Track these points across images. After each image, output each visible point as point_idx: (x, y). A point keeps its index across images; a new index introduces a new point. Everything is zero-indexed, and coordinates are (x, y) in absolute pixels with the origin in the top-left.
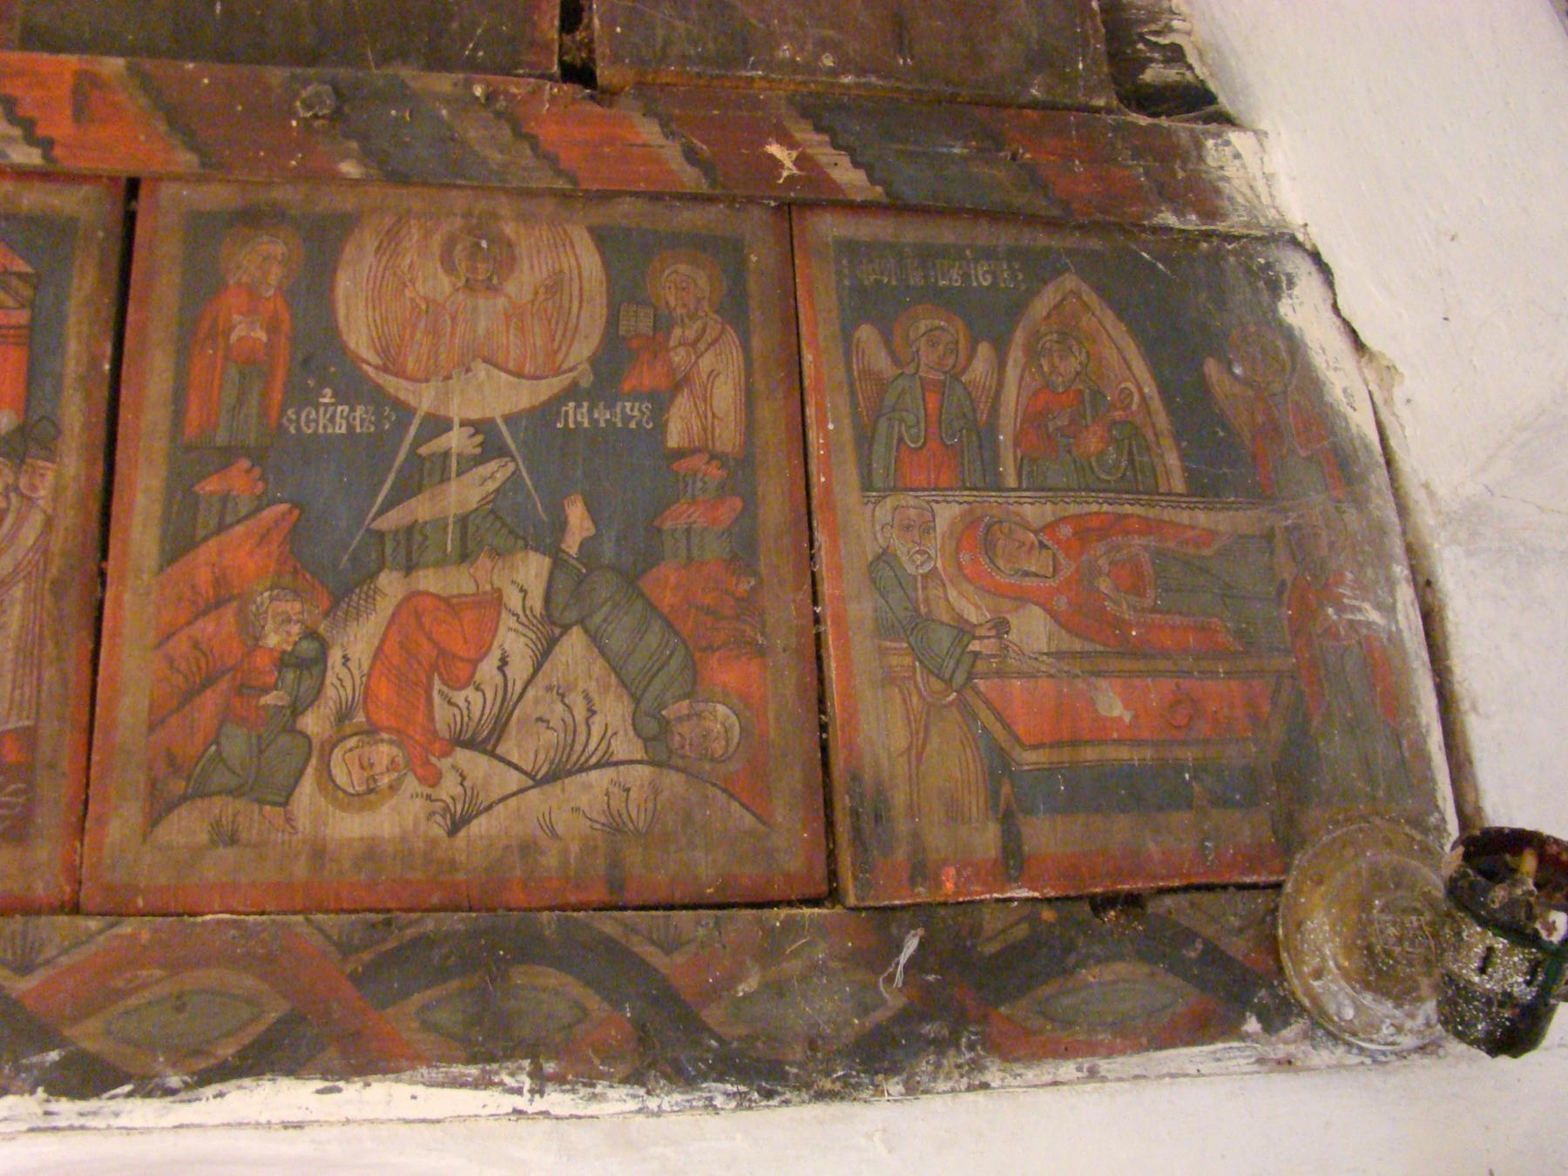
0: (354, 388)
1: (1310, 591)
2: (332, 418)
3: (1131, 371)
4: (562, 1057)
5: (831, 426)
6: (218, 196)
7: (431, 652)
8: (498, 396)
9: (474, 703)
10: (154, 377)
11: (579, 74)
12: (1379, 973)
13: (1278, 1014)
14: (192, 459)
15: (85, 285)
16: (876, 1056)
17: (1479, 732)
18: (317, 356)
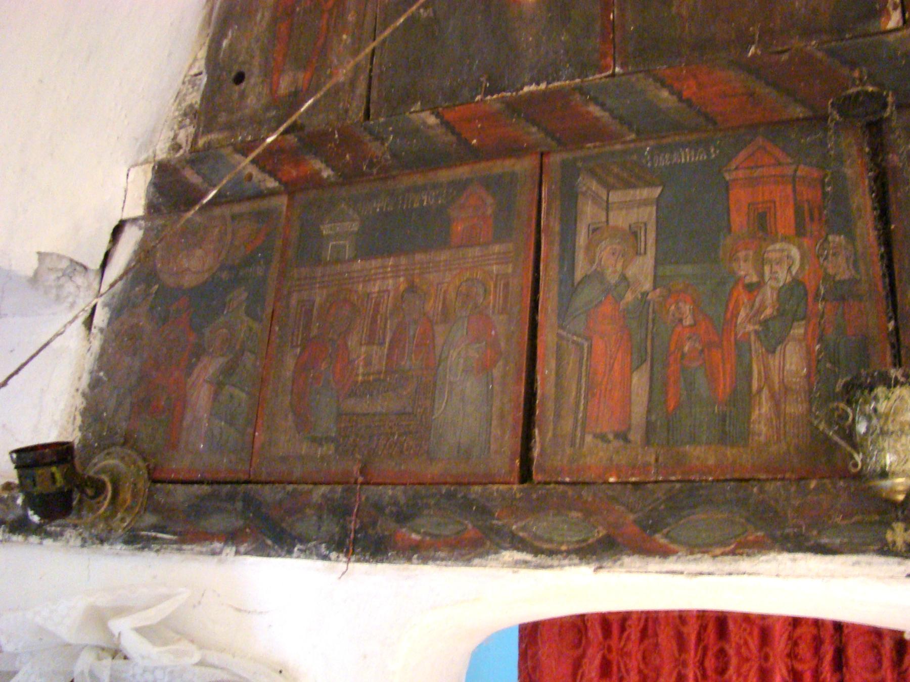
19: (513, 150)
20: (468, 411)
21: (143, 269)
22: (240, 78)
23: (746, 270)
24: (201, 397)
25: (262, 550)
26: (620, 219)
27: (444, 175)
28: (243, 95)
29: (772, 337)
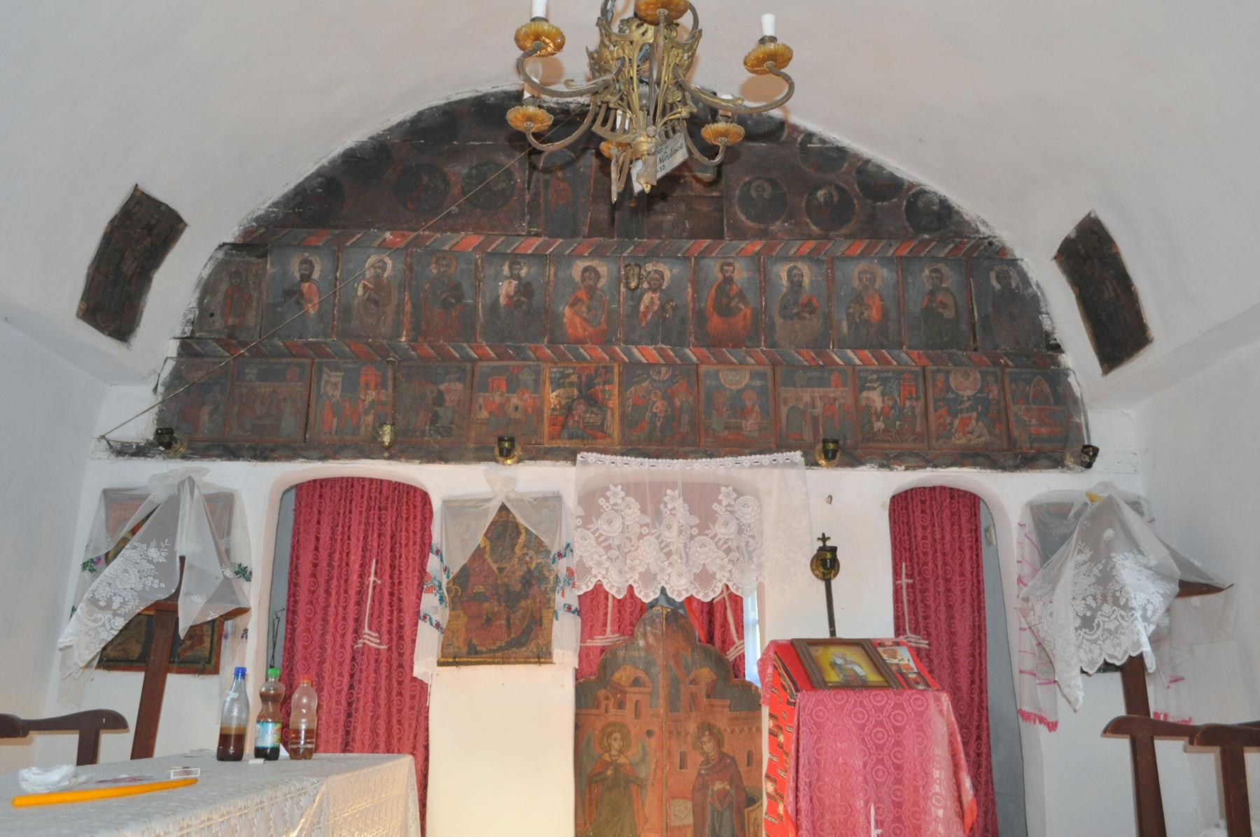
0: (953, 392)
1: (1070, 417)
2: (951, 396)
3: (1047, 389)
4: (983, 466)
5: (1009, 397)
6: (935, 368)
7: (965, 423)
8: (969, 393)
9: (970, 429)
10: (931, 391)
11: (975, 350)
12: (1076, 463)
13: (1063, 466)
14: (935, 402)
15: (920, 380)
16: (1016, 468)
17: (1092, 435)
18: (948, 388)
20: (290, 425)
21: (177, 375)
22: (212, 315)
23: (362, 397)
24: (205, 417)
26: (333, 380)
27: (284, 360)
29: (366, 413)
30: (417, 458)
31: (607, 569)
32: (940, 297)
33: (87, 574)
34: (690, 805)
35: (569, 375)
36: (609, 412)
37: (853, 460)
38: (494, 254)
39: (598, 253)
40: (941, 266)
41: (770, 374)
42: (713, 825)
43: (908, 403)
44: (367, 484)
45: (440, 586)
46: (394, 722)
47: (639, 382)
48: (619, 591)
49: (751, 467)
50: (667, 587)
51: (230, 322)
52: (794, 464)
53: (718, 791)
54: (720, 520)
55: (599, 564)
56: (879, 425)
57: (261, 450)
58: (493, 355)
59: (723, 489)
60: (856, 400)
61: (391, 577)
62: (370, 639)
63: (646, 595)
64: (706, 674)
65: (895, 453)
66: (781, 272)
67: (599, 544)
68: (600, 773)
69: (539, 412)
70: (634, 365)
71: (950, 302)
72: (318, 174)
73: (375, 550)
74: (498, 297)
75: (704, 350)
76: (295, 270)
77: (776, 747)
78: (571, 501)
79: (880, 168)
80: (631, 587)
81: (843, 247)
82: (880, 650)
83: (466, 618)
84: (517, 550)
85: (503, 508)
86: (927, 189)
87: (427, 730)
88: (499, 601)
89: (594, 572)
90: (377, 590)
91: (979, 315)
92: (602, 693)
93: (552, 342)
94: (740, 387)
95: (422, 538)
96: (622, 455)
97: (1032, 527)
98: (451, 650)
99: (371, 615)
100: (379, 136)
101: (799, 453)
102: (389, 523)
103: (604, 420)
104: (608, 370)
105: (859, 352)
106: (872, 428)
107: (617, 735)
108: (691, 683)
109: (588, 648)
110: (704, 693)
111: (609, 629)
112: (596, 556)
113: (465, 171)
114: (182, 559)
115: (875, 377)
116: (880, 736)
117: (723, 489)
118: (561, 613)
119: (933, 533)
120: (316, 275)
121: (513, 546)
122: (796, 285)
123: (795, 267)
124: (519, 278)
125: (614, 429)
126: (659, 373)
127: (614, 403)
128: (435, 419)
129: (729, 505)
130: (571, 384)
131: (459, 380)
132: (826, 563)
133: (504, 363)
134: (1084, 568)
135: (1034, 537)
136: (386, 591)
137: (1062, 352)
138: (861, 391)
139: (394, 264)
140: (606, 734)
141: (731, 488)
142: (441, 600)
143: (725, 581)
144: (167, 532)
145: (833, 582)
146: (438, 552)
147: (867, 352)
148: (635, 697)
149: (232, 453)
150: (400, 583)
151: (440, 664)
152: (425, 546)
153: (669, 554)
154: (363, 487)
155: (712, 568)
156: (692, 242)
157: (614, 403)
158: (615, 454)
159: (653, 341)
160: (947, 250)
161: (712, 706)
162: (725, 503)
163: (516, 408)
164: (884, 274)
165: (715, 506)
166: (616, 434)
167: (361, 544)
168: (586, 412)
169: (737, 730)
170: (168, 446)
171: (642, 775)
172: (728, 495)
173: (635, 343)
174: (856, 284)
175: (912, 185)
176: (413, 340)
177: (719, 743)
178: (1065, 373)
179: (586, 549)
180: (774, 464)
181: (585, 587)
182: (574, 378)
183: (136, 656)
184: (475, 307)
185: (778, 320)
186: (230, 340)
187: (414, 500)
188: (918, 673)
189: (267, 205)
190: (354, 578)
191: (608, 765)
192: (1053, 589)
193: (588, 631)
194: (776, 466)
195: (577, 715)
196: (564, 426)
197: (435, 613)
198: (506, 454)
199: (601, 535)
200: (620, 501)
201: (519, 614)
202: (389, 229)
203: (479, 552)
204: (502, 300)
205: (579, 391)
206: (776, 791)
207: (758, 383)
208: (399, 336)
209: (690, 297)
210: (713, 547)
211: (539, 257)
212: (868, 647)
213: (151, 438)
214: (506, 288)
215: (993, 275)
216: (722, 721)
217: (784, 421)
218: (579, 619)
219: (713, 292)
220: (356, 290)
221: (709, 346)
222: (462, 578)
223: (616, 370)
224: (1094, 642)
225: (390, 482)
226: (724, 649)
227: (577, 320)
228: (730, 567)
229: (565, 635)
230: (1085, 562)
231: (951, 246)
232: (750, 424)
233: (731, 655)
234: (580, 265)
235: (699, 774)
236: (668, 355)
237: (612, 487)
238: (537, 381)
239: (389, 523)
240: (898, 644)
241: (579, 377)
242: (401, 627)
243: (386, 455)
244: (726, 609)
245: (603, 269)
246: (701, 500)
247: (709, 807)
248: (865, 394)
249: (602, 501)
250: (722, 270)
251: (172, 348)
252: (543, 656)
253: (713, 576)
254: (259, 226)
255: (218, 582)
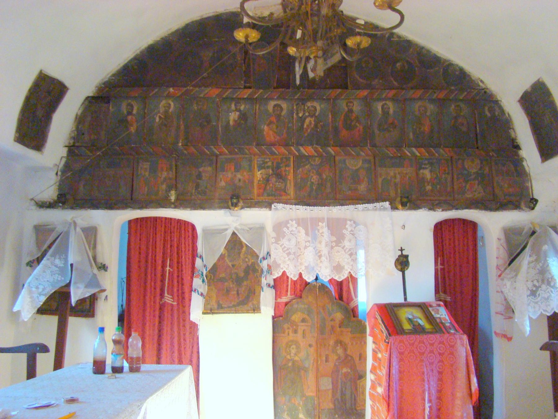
0: (466, 169)
2: (465, 172)
4: (481, 209)
5: (494, 172)
7: (472, 186)
8: (475, 171)
11: (478, 148)
12: (526, 207)
16: (496, 209)
17: (534, 192)
18: (463, 168)
19: (131, 154)
20: (124, 191)
22: (83, 134)
23: (160, 175)
24: (81, 188)
25: (94, 209)
28: (84, 137)
29: (162, 184)
30: (189, 208)
31: (288, 265)
32: (460, 120)
33: (29, 268)
34: (330, 380)
35: (267, 162)
36: (288, 181)
37: (415, 206)
38: (226, 98)
39: (282, 97)
40: (460, 103)
41: (372, 160)
42: (342, 389)
43: (443, 176)
44: (164, 220)
45: (203, 275)
46: (182, 340)
47: (304, 166)
48: (294, 276)
49: (363, 210)
50: (319, 273)
51: (93, 137)
52: (385, 209)
53: (345, 373)
54: (347, 238)
55: (284, 262)
56: (429, 188)
57: (110, 204)
58: (227, 152)
59: (348, 222)
60: (417, 175)
61: (178, 268)
62: (168, 299)
63: (309, 278)
64: (339, 316)
65: (437, 202)
66: (378, 107)
67: (284, 252)
68: (285, 365)
69: (252, 182)
70: (302, 156)
71: (465, 123)
72: (135, 58)
73: (169, 254)
74: (229, 121)
75: (338, 148)
76: (124, 109)
77: (375, 358)
78: (269, 228)
79: (429, 51)
80: (300, 275)
81: (411, 94)
82: (430, 309)
83: (216, 291)
84: (242, 256)
85: (234, 234)
86: (453, 63)
87: (198, 344)
88: (232, 281)
89: (281, 266)
90: (171, 274)
91: (480, 129)
92: (286, 326)
93: (258, 145)
94: (356, 168)
95: (193, 247)
96: (296, 204)
97: (504, 240)
98: (209, 307)
99: (168, 287)
100: (166, 37)
101: (387, 203)
102: (175, 240)
103: (286, 186)
104: (288, 159)
105: (418, 149)
106: (425, 189)
107: (294, 346)
108: (331, 321)
109: (279, 303)
110: (338, 326)
111: (289, 293)
112: (282, 258)
113: (210, 55)
114: (72, 265)
115: (426, 162)
116: (431, 358)
117: (348, 222)
118: (265, 288)
119: (454, 242)
120: (135, 112)
121: (240, 253)
122: (385, 113)
123: (386, 104)
124: (240, 111)
125: (291, 191)
126: (315, 161)
127: (291, 177)
128: (197, 186)
129: (352, 231)
130: (268, 167)
131: (210, 165)
132: (403, 263)
133: (233, 156)
134: (532, 265)
135: (505, 245)
136: (175, 275)
137: (520, 149)
138: (420, 170)
139: (175, 106)
140: (288, 345)
141: (352, 222)
142: (203, 281)
143: (349, 270)
144: (63, 251)
145: (406, 272)
146: (201, 257)
147: (423, 149)
148: (303, 328)
149: (95, 205)
150: (182, 271)
151: (204, 313)
152: (194, 255)
153: (320, 257)
154: (162, 221)
155: (343, 264)
156: (331, 91)
157: (291, 177)
158: (291, 204)
159: (312, 145)
160: (464, 95)
161: (342, 331)
162: (349, 230)
163: (240, 180)
164: (431, 108)
165: (344, 231)
166: (292, 193)
167: (162, 251)
168: (276, 182)
169: (354, 343)
170: (64, 203)
171: (307, 366)
172: (351, 225)
173: (302, 145)
174: (417, 113)
175: (445, 61)
176: (185, 145)
177: (345, 350)
178: (521, 160)
179: (277, 254)
180: (375, 209)
181: (277, 274)
182: (270, 164)
183: (54, 308)
184: (218, 126)
185: (376, 131)
186: (93, 146)
187: (188, 229)
188: (451, 323)
189: (109, 75)
190: (159, 268)
191: (289, 360)
192: (516, 275)
193: (277, 296)
194: (376, 210)
195: (274, 336)
196: (265, 189)
197: (200, 288)
198: (235, 205)
199: (285, 247)
200: (294, 229)
201: (243, 289)
202: (171, 87)
203: (222, 257)
204: (231, 123)
205: (273, 170)
206: (376, 379)
207: (367, 166)
208: (178, 143)
209: (330, 120)
210: (343, 252)
211: (250, 99)
212: (423, 307)
213: (56, 198)
214: (233, 116)
215: (486, 108)
216: (347, 339)
217: (380, 185)
218: (274, 291)
219: (342, 117)
220: (155, 119)
221: (340, 146)
222: (214, 270)
223: (292, 159)
224: (536, 303)
225: (175, 219)
226: (348, 304)
227: (271, 133)
228: (352, 263)
229: (267, 298)
230: (532, 262)
231: (465, 93)
232: (362, 188)
233: (352, 305)
234: (272, 103)
235: (335, 364)
236: (320, 152)
237: (290, 221)
238: (250, 166)
239: (175, 240)
240: (439, 305)
241: (273, 163)
242: (183, 293)
243: (173, 206)
244: (349, 282)
245: (284, 105)
246: (336, 228)
247: (340, 381)
248: (421, 171)
249: (285, 229)
250: (347, 106)
251: (64, 152)
252: (256, 309)
253: (343, 268)
254: (106, 87)
255: (90, 276)
